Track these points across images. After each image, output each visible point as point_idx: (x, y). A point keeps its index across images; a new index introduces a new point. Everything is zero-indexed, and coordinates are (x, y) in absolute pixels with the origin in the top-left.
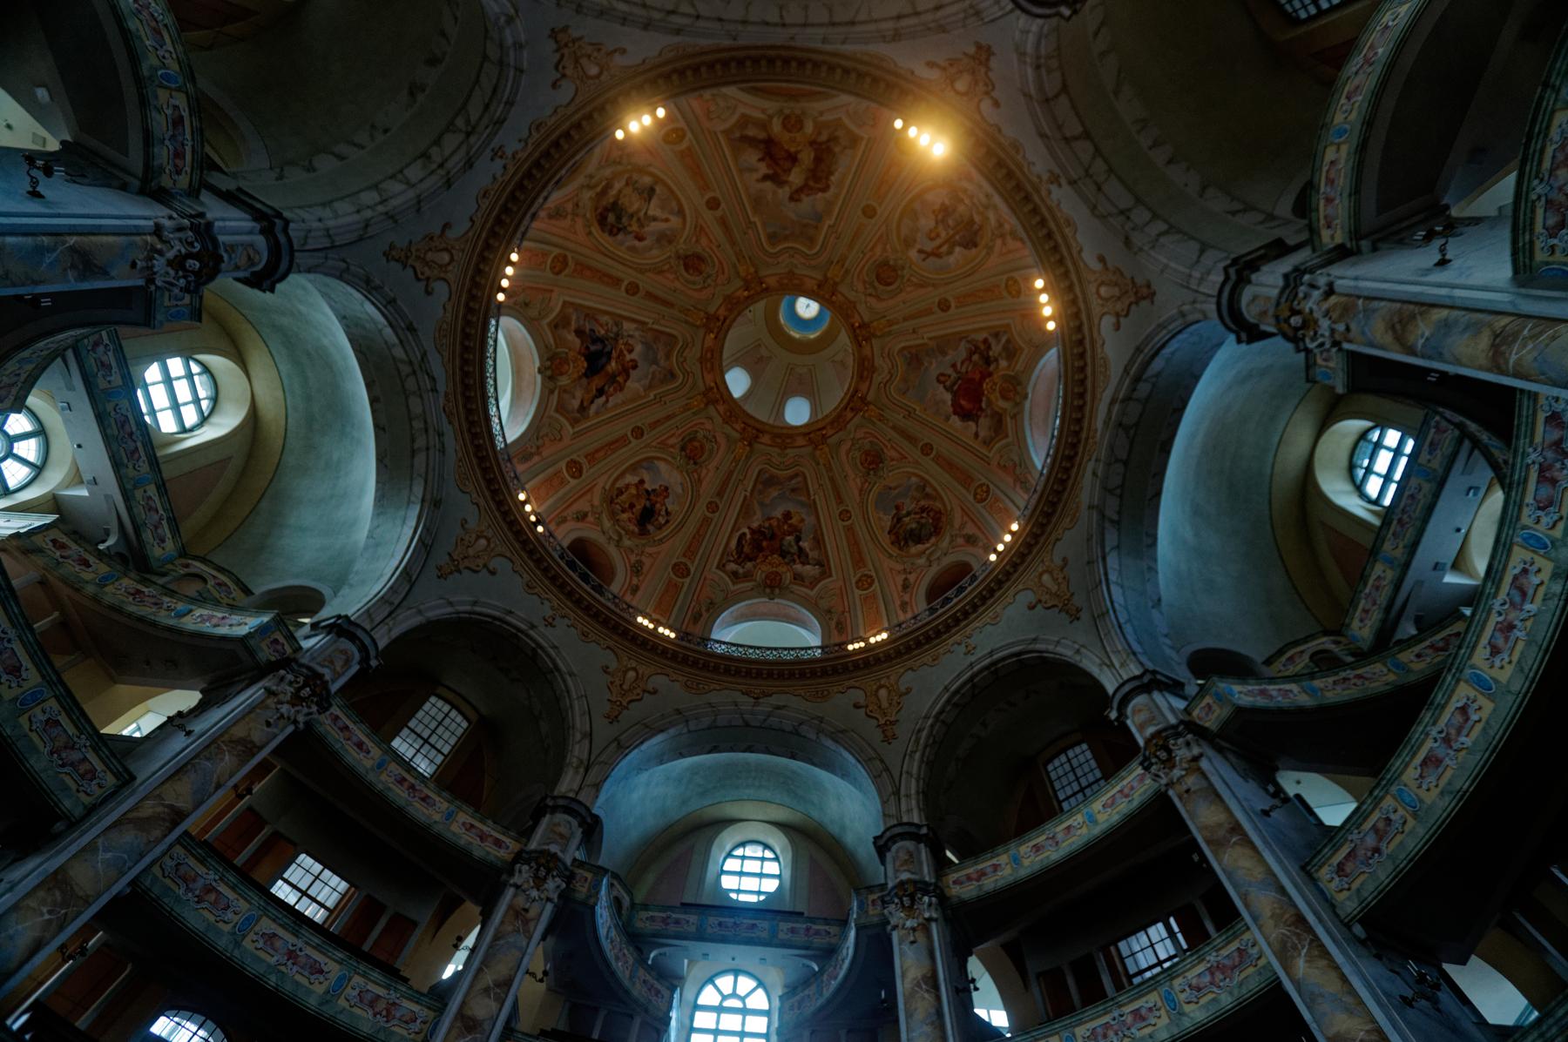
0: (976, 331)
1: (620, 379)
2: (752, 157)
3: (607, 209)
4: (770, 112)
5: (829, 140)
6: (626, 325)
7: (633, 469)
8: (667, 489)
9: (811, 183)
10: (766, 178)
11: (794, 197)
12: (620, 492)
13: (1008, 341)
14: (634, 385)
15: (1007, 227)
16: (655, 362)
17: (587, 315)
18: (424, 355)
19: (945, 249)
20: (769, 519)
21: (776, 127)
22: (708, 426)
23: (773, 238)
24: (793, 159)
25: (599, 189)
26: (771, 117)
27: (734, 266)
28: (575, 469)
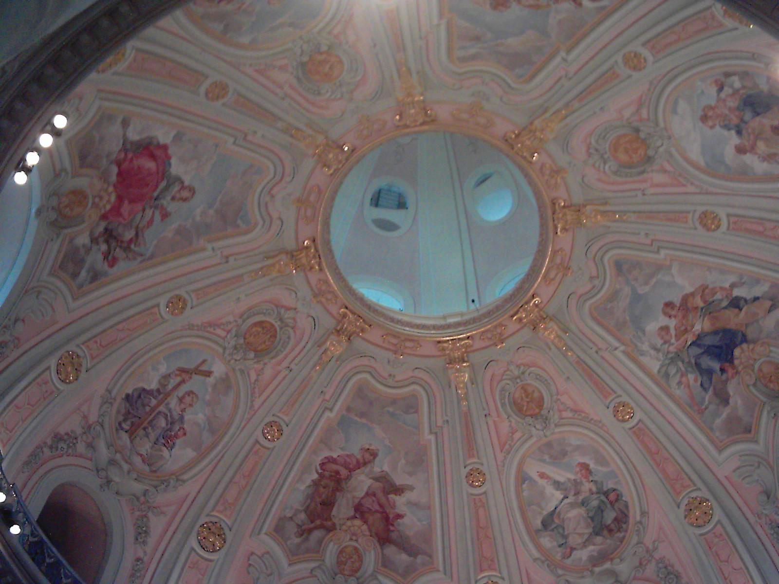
0: (129, 274)
2: (410, 524)
3: (610, 531)
5: (310, 531)
7: (744, 174)
8: (704, 118)
9: (344, 472)
10: (399, 490)
13: (75, 275)
14: (682, 283)
16: (637, 298)
17: (701, 412)
19: (173, 382)
21: (371, 559)
23: (411, 406)
25: (607, 565)
26: (373, 576)
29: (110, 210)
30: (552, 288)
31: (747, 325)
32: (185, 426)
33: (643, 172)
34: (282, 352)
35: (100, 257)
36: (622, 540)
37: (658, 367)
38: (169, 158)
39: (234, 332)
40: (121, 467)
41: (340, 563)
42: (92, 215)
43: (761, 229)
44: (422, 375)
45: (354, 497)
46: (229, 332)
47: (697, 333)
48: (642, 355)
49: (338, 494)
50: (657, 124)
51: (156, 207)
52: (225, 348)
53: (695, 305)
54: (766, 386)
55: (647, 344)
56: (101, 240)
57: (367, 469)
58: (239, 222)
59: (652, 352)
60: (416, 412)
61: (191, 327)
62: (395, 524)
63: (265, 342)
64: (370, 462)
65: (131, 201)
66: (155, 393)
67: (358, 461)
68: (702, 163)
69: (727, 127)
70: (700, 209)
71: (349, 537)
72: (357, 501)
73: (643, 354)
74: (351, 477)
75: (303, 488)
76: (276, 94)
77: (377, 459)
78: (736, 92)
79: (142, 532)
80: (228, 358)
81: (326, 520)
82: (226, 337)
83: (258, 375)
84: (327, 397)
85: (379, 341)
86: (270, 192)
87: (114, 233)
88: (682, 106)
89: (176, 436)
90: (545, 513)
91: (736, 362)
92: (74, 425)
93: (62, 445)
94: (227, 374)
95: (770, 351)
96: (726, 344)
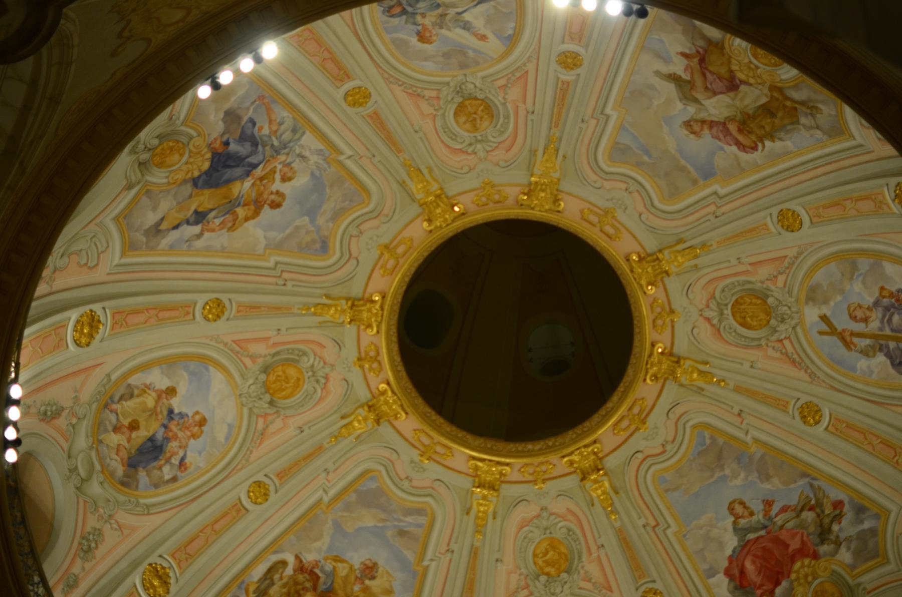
1: (241, 212)
5: (803, 103)
9: (733, 128)
10: (674, 78)
13: (873, 532)
14: (256, 231)
16: (312, 213)
20: (337, 559)
22: (330, 353)
23: (619, 152)
24: (732, 85)
27: (533, 153)
29: (807, 556)
30: (406, 233)
31: (191, 196)
32: (877, 295)
33: (274, 355)
34: (738, 282)
35: (844, 522)
37: (304, 138)
38: (730, 559)
39: (774, 338)
43: (161, 315)
44: (594, 177)
45: (733, 99)
46: (780, 341)
47: (249, 178)
48: (321, 150)
49: (751, 112)
50: (250, 410)
51: (770, 519)
52: (794, 328)
53: (246, 208)
54: (177, 141)
55: (311, 162)
56: (832, 537)
57: (703, 115)
58: (708, 442)
59: (306, 153)
60: (618, 143)
61: (812, 375)
62: (694, 51)
63: (750, 303)
64: (696, 121)
65: (787, 546)
66: (885, 351)
67: (711, 128)
68: (212, 369)
69: (182, 415)
71: (759, 71)
72: (732, 94)
73: (319, 152)
74: (726, 118)
75: (788, 143)
76: (607, 555)
77: (686, 119)
78: (168, 461)
80: (796, 316)
81: (777, 100)
82: (785, 338)
83: (776, 277)
84: (712, 208)
86: (665, 451)
88: (221, 436)
89: (891, 295)
91: (209, 155)
94: (807, 303)
95: (167, 177)
96: (218, 171)
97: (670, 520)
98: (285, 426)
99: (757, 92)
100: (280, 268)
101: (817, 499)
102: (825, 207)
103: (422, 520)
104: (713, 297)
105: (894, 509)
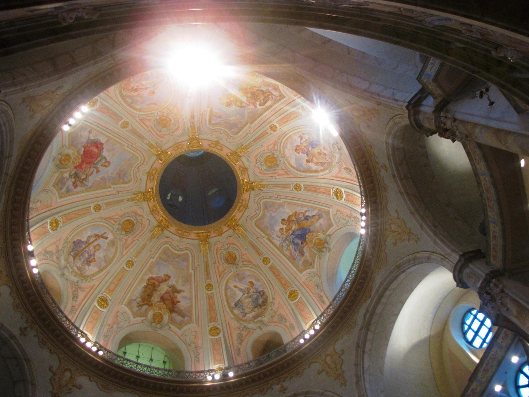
2: (183, 305)
3: (260, 306)
4: (167, 327)
5: (142, 305)
6: (278, 243)
7: (309, 171)
8: (296, 150)
9: (157, 283)
10: (179, 292)
11: (168, 277)
12: (322, 164)
13: (61, 189)
14: (287, 212)
15: (55, 258)
18: (360, 330)
19: (93, 239)
21: (166, 318)
23: (185, 258)
25: (260, 319)
26: (167, 324)
27: (210, 250)
28: (338, 194)
30: (241, 214)
33: (275, 170)
35: (72, 183)
36: (265, 309)
38: (103, 148)
40: (69, 270)
41: (154, 319)
42: (71, 165)
43: (314, 189)
46: (116, 222)
49: (154, 292)
51: (95, 168)
52: (114, 229)
56: (73, 176)
57: (166, 283)
58: (125, 178)
59: (277, 238)
64: (168, 280)
65: (86, 164)
69: (303, 153)
70: (295, 183)
72: (162, 295)
75: (140, 288)
77: (171, 279)
79: (75, 297)
84: (152, 253)
85: (174, 232)
87: (78, 175)
89: (91, 261)
90: (236, 301)
91: (307, 240)
92: (53, 249)
93: (47, 255)
97: (128, 149)
98: (268, 147)
99: (155, 300)
100: (279, 198)
101: (83, 183)
102: (122, 276)
103: (213, 122)
104: (141, 224)
105: (59, 200)
